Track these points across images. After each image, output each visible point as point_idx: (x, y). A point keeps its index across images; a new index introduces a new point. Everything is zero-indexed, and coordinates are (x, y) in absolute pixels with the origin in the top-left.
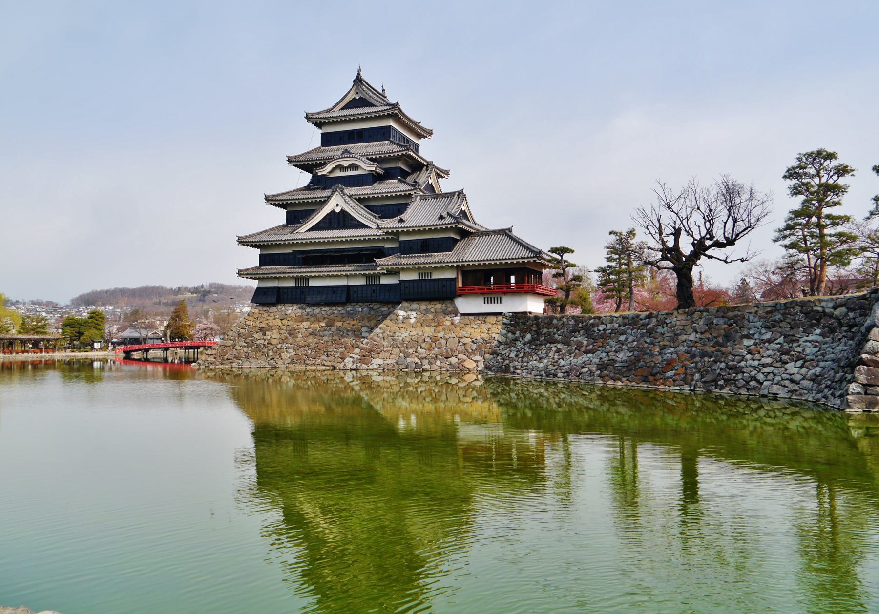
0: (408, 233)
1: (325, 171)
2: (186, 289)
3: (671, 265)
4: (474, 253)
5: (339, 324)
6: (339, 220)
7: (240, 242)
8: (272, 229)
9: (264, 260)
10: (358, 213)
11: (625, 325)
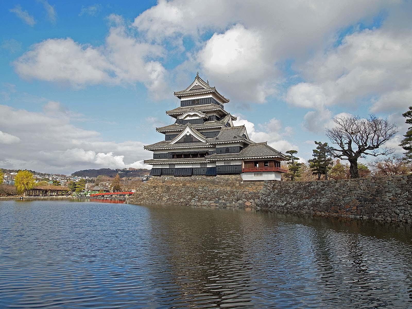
0: (220, 144)
2: (119, 170)
3: (347, 158)
4: (249, 154)
5: (188, 185)
6: (188, 139)
7: (145, 148)
9: (155, 156)
10: (197, 136)
11: (324, 186)
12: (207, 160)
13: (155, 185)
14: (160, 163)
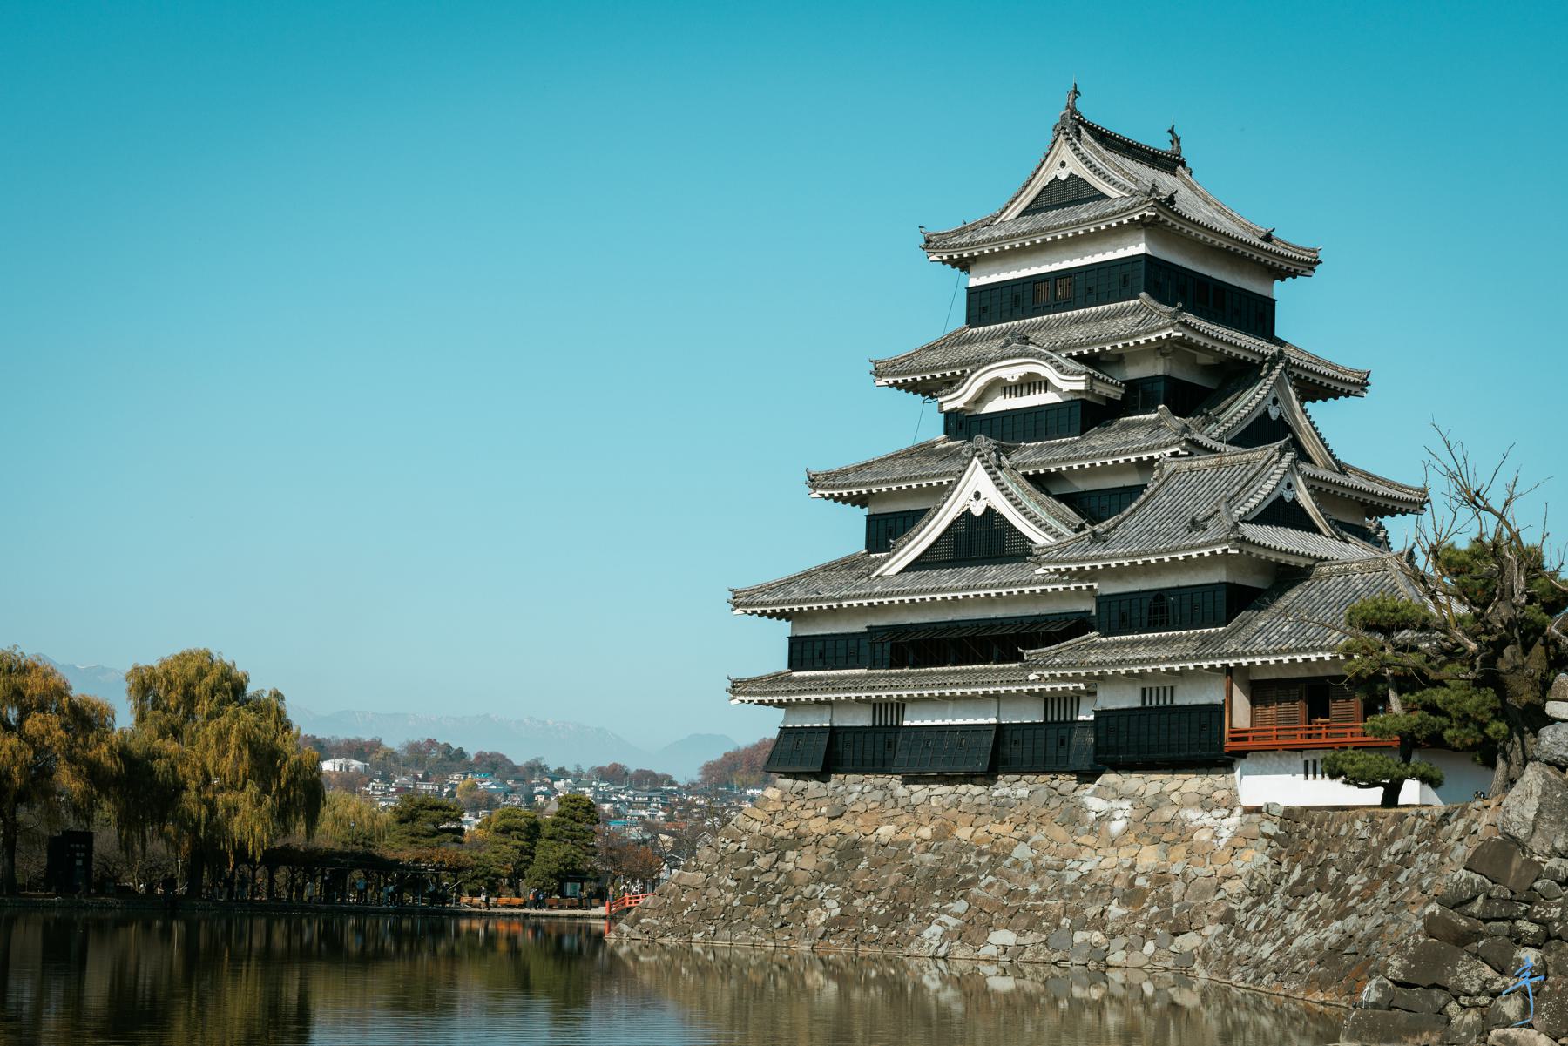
1: (957, 400)
5: (963, 833)
6: (981, 540)
7: (737, 606)
8: (827, 568)
9: (803, 653)
12: (1032, 677)
13: (783, 833)
14: (813, 697)
